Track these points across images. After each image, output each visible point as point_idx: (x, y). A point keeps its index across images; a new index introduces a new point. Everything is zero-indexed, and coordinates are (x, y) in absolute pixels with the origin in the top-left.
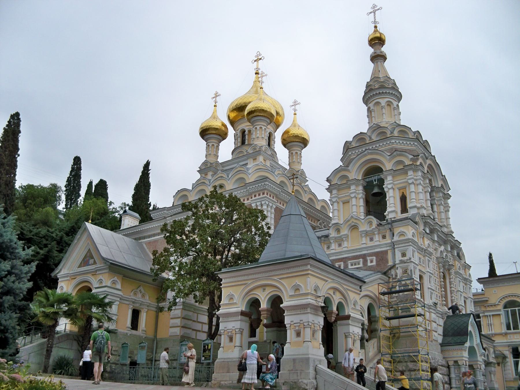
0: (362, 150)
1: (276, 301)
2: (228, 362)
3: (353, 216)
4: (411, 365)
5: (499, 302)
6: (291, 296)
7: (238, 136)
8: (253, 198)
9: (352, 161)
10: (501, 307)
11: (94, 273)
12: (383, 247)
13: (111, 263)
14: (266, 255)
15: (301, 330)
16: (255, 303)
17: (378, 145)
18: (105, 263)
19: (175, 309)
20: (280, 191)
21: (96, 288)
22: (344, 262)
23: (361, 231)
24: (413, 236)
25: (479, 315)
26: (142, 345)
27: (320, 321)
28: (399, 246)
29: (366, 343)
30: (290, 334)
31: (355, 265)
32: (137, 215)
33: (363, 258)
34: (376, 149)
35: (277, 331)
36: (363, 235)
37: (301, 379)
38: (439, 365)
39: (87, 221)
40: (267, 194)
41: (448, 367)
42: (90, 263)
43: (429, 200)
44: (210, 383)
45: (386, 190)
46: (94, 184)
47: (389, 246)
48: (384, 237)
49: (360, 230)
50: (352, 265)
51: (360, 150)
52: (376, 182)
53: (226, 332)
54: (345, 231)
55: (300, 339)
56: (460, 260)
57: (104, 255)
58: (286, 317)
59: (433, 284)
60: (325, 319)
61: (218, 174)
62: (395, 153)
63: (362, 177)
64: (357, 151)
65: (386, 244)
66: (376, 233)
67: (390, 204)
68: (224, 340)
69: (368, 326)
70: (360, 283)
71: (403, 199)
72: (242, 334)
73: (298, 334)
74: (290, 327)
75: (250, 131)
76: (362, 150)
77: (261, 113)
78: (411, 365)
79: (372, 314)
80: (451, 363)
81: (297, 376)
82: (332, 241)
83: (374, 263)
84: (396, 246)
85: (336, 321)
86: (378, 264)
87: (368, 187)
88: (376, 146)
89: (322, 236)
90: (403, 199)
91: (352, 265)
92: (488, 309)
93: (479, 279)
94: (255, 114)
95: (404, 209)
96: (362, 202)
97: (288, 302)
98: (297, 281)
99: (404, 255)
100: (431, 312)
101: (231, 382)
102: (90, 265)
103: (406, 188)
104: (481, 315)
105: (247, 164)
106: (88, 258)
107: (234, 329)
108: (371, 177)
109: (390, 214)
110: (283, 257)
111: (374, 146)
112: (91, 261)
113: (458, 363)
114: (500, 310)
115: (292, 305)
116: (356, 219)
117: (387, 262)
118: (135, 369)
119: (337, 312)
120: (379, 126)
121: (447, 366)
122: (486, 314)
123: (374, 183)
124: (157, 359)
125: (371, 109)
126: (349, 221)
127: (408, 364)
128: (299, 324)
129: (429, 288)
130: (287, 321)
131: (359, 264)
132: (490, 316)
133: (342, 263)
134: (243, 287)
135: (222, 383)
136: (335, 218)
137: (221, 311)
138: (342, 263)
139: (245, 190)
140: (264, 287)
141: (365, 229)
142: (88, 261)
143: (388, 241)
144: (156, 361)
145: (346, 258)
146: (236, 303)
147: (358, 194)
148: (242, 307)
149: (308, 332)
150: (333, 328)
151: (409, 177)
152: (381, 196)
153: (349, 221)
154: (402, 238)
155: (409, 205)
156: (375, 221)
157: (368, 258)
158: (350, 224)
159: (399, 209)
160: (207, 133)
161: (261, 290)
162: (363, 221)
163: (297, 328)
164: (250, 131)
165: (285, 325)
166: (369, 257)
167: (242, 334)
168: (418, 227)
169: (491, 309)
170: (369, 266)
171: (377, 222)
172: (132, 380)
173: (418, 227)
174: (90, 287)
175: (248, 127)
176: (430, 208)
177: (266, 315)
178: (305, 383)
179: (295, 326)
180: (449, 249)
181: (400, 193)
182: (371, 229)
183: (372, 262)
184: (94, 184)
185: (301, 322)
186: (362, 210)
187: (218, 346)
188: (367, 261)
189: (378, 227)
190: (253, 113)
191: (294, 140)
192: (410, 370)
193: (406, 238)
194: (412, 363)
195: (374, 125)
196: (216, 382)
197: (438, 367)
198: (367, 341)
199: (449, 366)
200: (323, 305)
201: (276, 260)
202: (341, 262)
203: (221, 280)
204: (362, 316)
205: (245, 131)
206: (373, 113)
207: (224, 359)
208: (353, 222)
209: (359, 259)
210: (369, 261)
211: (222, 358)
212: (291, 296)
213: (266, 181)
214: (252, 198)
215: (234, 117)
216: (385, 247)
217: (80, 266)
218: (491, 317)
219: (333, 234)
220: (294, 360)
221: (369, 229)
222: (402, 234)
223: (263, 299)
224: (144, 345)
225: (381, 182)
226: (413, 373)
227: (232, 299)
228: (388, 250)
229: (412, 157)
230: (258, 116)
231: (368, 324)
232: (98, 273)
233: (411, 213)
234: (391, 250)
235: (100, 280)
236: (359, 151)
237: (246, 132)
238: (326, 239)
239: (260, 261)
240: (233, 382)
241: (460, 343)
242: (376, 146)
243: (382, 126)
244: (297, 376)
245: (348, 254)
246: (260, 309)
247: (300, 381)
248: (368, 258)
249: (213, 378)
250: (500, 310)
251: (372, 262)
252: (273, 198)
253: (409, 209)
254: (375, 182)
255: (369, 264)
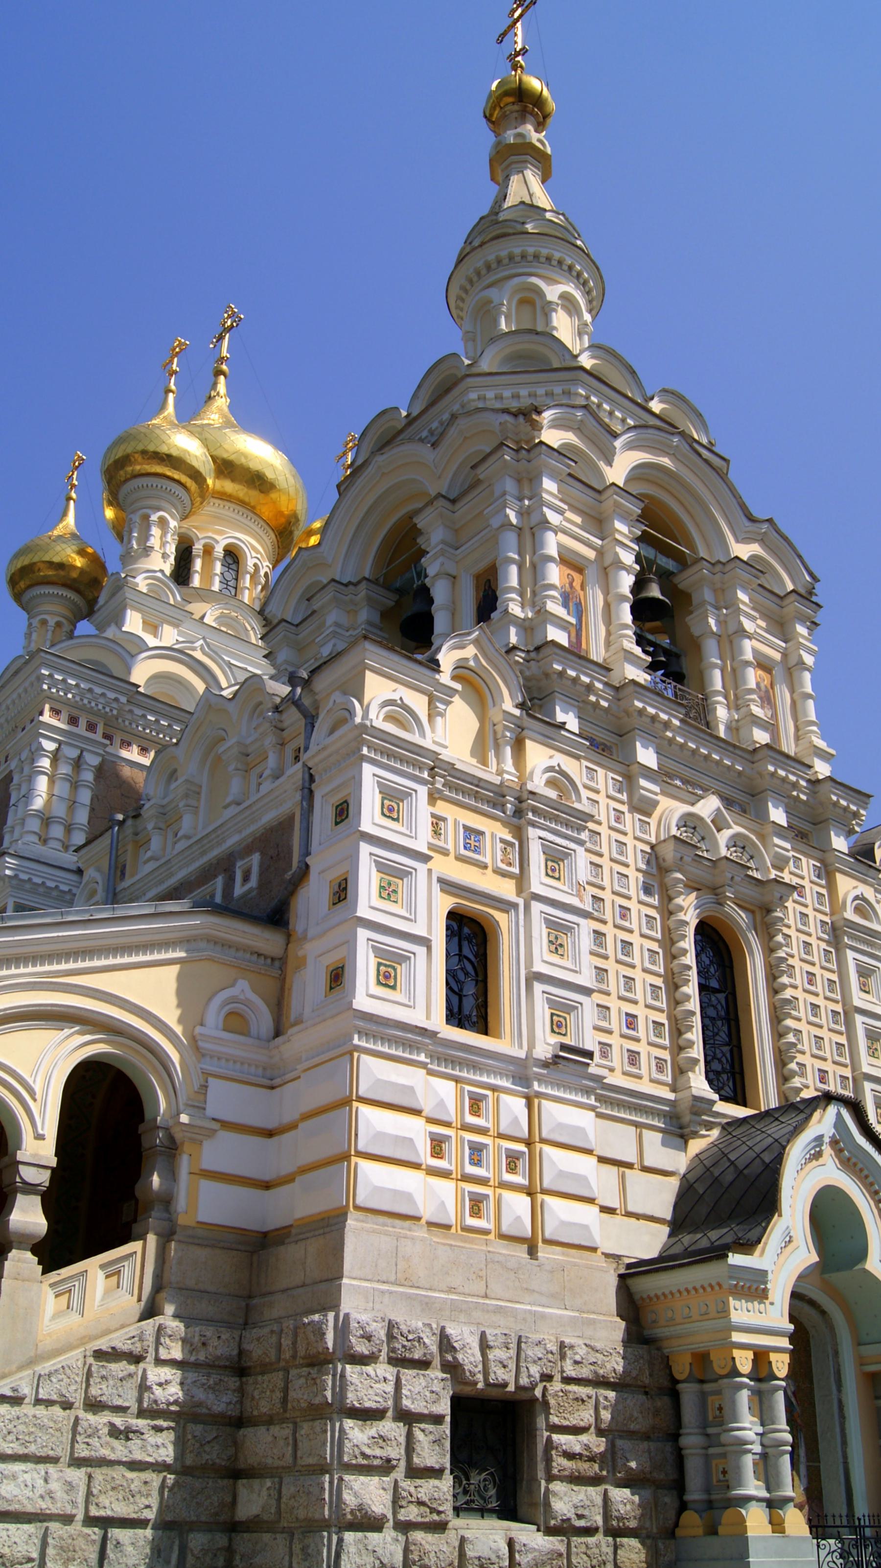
20: (123, 699)
33: (225, 870)
80: (682, 1368)
83: (253, 882)
100: (539, 1095)
121: (666, 1383)
183: (246, 878)
199: (675, 1382)
209: (216, 876)
251: (246, 878)
252: (91, 727)
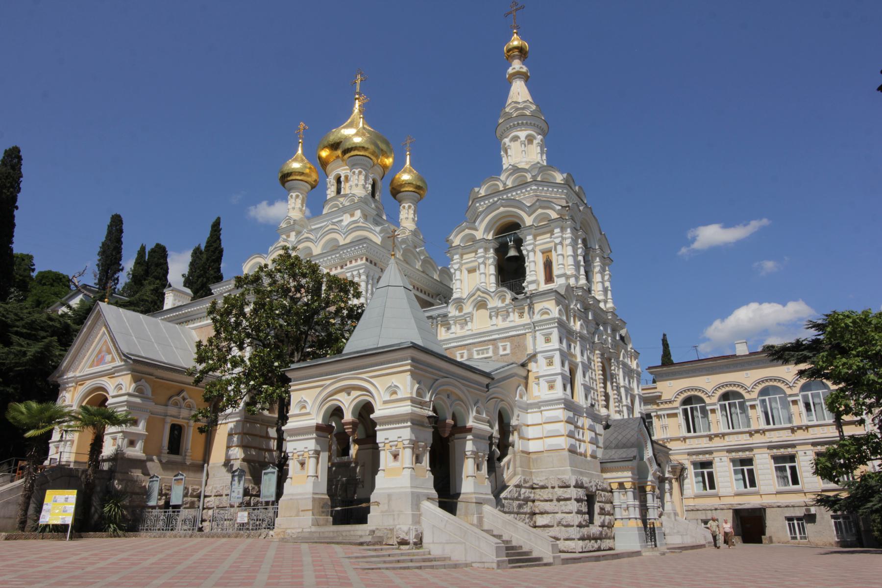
0: (493, 200)
1: (366, 409)
2: (297, 499)
3: (481, 288)
4: (560, 492)
5: (676, 397)
6: (385, 402)
7: (331, 183)
8: (349, 265)
9: (481, 214)
10: (677, 404)
11: (111, 374)
12: (520, 330)
13: (134, 360)
14: (355, 343)
15: (399, 451)
16: (337, 412)
17: (514, 193)
18: (125, 361)
19: (221, 424)
21: (113, 397)
22: (468, 350)
23: (491, 309)
24: (559, 314)
25: (650, 414)
26: (179, 477)
27: (428, 435)
28: (542, 328)
29: (497, 464)
30: (385, 458)
31: (483, 354)
32: (188, 291)
34: (512, 198)
35: (372, 448)
36: (493, 314)
37: (399, 524)
38: (599, 490)
39: (102, 300)
40: (367, 260)
41: (611, 491)
42: (106, 361)
43: (582, 265)
44: (271, 532)
45: (525, 252)
46: (148, 250)
47: (528, 328)
48: (521, 315)
49: (488, 307)
50: (478, 354)
51: (491, 201)
52: (512, 243)
53: (296, 456)
54: (468, 308)
55: (397, 464)
56: (625, 345)
57: (125, 351)
58: (378, 433)
59: (587, 379)
60: (437, 436)
61: (303, 234)
62: (537, 204)
63: (493, 236)
64: (487, 202)
65: (524, 325)
66: (510, 310)
67: (531, 272)
68: (293, 466)
69: (499, 439)
70: (486, 381)
71: (548, 266)
72: (318, 459)
73: (396, 456)
74: (384, 446)
75: (346, 177)
76: (493, 200)
77: (360, 151)
78: (560, 492)
79: (505, 421)
81: (394, 519)
82: (451, 322)
83: (508, 351)
84: (537, 328)
85: (452, 434)
86: (513, 353)
87: (501, 250)
88: (512, 195)
89: (439, 316)
90: (548, 266)
91: (478, 354)
92: (662, 406)
93: (650, 368)
94: (353, 153)
95: (549, 278)
96: (492, 270)
97: (381, 411)
98: (393, 381)
99: (548, 340)
101: (300, 530)
102: (106, 363)
103: (551, 251)
104: (653, 414)
105: (342, 221)
106: (103, 354)
107: (306, 450)
108: (505, 236)
109: (529, 286)
110: (375, 346)
111: (509, 195)
112: (108, 358)
113: (624, 485)
114: (677, 408)
115: (387, 415)
116: (483, 292)
117: (526, 349)
118: (167, 514)
119: (452, 422)
120: (516, 168)
122: (659, 413)
123: (510, 244)
124: (206, 494)
125: (507, 145)
126: (474, 295)
127: (557, 489)
128: (396, 443)
129: (582, 384)
130: (380, 437)
131: (487, 353)
132: (664, 415)
133: (465, 351)
134: (321, 389)
135: (289, 531)
136: (458, 290)
137: (290, 425)
138: (465, 351)
139: (337, 255)
140: (348, 390)
141: (495, 306)
142: (103, 357)
143: (526, 319)
144: (205, 496)
145: (470, 344)
146: (308, 414)
147: (489, 258)
148: (317, 419)
149: (407, 456)
150: (449, 444)
151: (556, 235)
152: (520, 260)
153: (474, 295)
154: (545, 317)
155: (556, 271)
156: (509, 295)
157: (500, 344)
158: (476, 299)
159: (541, 277)
160: (289, 179)
161: (344, 394)
162: (492, 294)
163: (394, 448)
164: (346, 177)
165: (377, 444)
166: (501, 342)
167: (318, 459)
168: (567, 302)
169: (666, 406)
170: (501, 356)
171: (511, 294)
172: (163, 530)
173: (567, 302)
174: (105, 396)
175: (344, 172)
176: (584, 277)
177: (351, 430)
178: (404, 532)
179: (391, 446)
180: (609, 332)
181: (543, 257)
182: (504, 305)
183: (505, 349)
184: (148, 250)
185: (400, 440)
186: (493, 279)
187: (282, 477)
188: (498, 348)
189: (513, 302)
190: (350, 151)
191: (407, 189)
192: (559, 500)
193: (551, 316)
194: (562, 489)
195: (510, 167)
196: (280, 531)
197: (597, 492)
198: (500, 459)
199: (612, 489)
200: (431, 413)
201: (366, 351)
202: (464, 349)
203: (289, 380)
204: (491, 427)
205: (340, 177)
206: (509, 150)
207: (292, 495)
208: (479, 296)
209: (488, 345)
210: (501, 349)
211: (289, 494)
212: (385, 402)
213: (365, 243)
214: (346, 265)
215: (327, 156)
216: (522, 330)
217: (91, 366)
218: (666, 417)
219: (452, 311)
220: (389, 496)
221: (499, 304)
222: (545, 312)
223: (347, 406)
224: (181, 477)
225: (519, 243)
226: (562, 503)
227: (304, 407)
228: (525, 334)
229: (560, 208)
230: (357, 155)
231: (499, 436)
232: (116, 374)
233: (558, 283)
234: (531, 334)
235: (118, 385)
236: (489, 202)
237: (342, 179)
238: (444, 319)
239: (344, 352)
240: (304, 530)
241: (626, 458)
242: (512, 195)
243: (520, 167)
244: (394, 519)
245: (472, 339)
246: (343, 421)
247: (398, 527)
248: (500, 344)
249: (276, 525)
250: (677, 408)
251: (505, 349)
253: (555, 278)
254: (511, 242)
255: (501, 352)
